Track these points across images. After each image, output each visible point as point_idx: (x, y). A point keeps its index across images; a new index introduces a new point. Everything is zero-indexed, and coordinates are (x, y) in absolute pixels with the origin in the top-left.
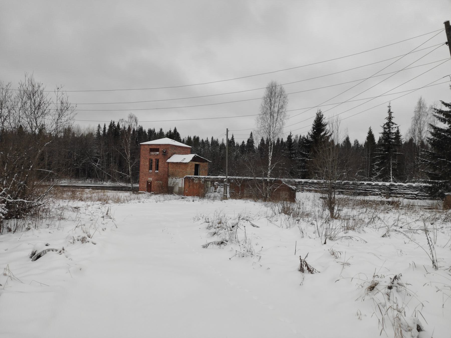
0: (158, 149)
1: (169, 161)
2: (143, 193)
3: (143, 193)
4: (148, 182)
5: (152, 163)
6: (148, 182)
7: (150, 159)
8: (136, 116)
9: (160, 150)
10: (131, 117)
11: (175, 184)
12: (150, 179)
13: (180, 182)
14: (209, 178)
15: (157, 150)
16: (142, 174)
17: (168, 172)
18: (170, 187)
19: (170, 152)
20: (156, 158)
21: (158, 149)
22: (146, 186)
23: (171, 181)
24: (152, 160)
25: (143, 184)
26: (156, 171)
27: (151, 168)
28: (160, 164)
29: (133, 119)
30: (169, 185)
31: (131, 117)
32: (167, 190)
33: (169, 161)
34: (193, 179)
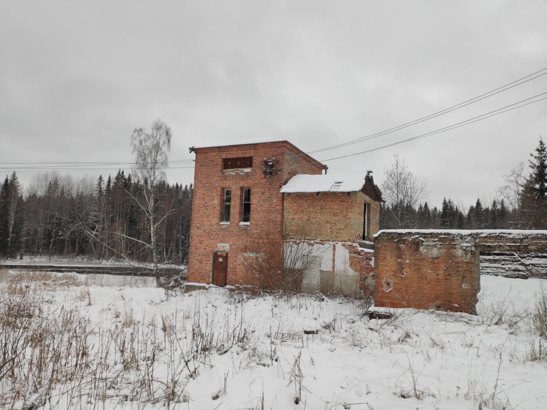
0: (250, 159)
1: (285, 189)
2: (200, 288)
3: (200, 288)
4: (216, 256)
5: (229, 200)
6: (216, 256)
7: (223, 189)
8: (169, 126)
9: (257, 161)
10: (158, 127)
11: (309, 262)
12: (224, 247)
13: (334, 257)
14: (499, 237)
15: (247, 162)
16: (199, 232)
17: (282, 222)
18: (292, 271)
19: (286, 167)
20: (242, 183)
21: (250, 159)
22: (210, 267)
23: (293, 253)
24: (228, 193)
25: (201, 262)
26: (242, 223)
27: (225, 214)
28: (254, 200)
29: (161, 132)
30: (288, 263)
31: (158, 127)
32: (277, 278)
33: (285, 189)
34: (417, 244)
